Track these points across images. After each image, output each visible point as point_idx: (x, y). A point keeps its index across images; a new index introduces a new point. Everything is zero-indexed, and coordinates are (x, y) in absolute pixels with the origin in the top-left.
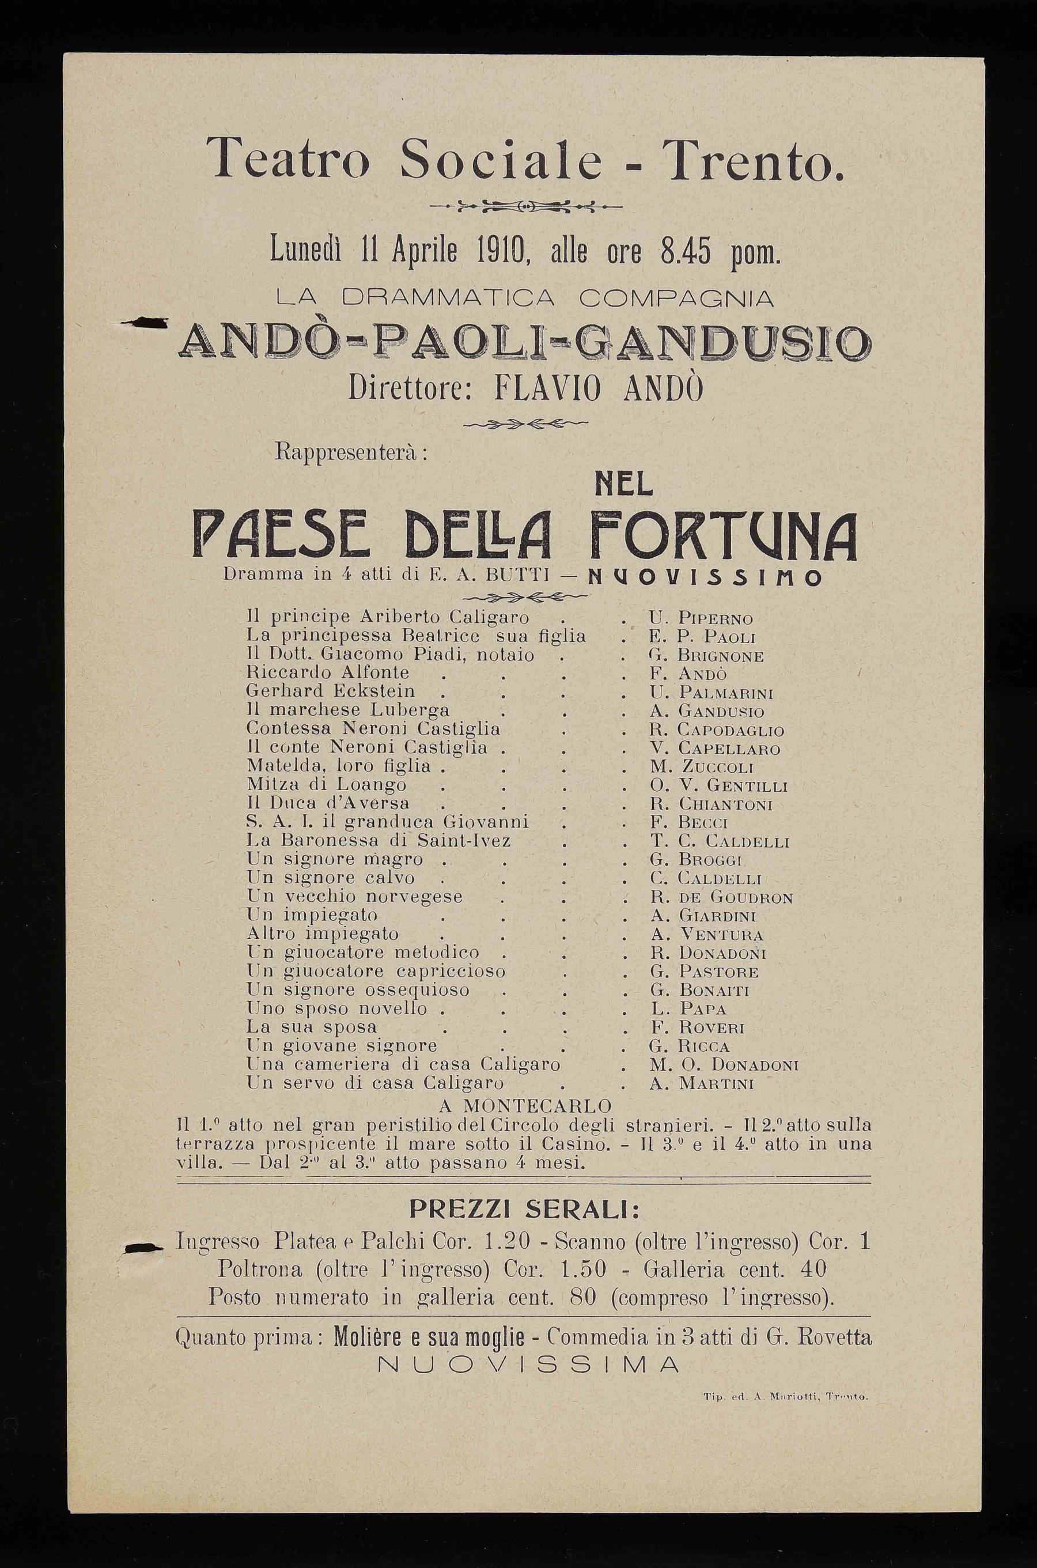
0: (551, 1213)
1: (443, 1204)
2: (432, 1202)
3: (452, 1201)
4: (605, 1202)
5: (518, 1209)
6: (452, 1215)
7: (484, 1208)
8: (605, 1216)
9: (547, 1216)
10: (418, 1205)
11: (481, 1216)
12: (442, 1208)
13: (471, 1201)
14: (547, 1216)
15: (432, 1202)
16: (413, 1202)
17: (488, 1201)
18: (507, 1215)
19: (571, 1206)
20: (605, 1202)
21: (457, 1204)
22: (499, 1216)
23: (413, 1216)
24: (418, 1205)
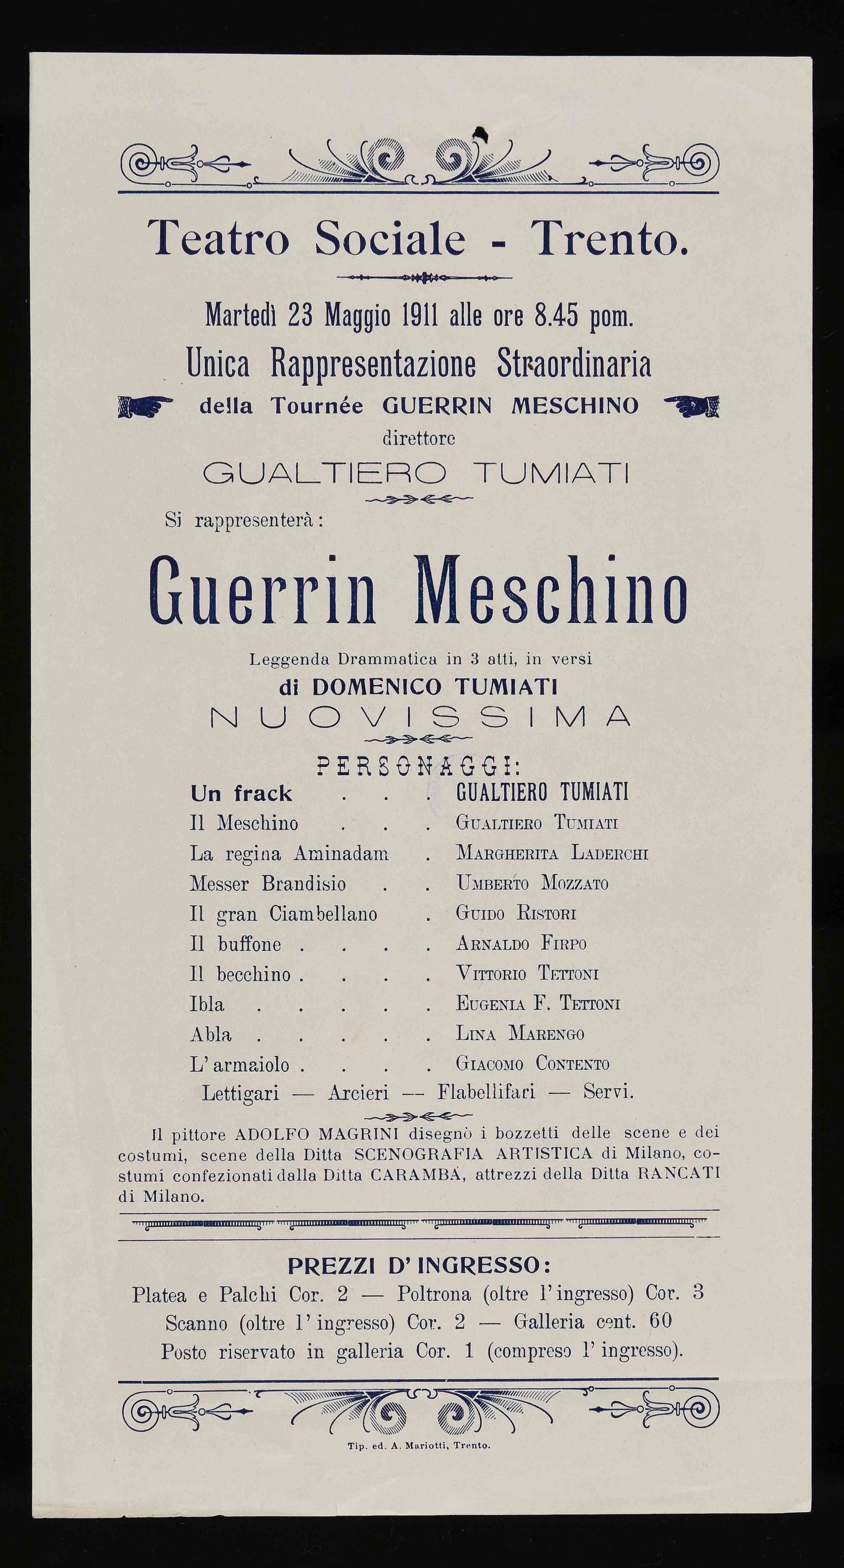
2: (307, 1260)
3: (325, 1260)
6: (325, 1272)
7: (353, 1266)
10: (295, 1263)
11: (350, 1272)
13: (341, 1259)
15: (307, 1260)
16: (291, 1260)
17: (356, 1259)
18: (372, 1271)
21: (329, 1262)
22: (365, 1272)
23: (291, 1272)
24: (295, 1263)
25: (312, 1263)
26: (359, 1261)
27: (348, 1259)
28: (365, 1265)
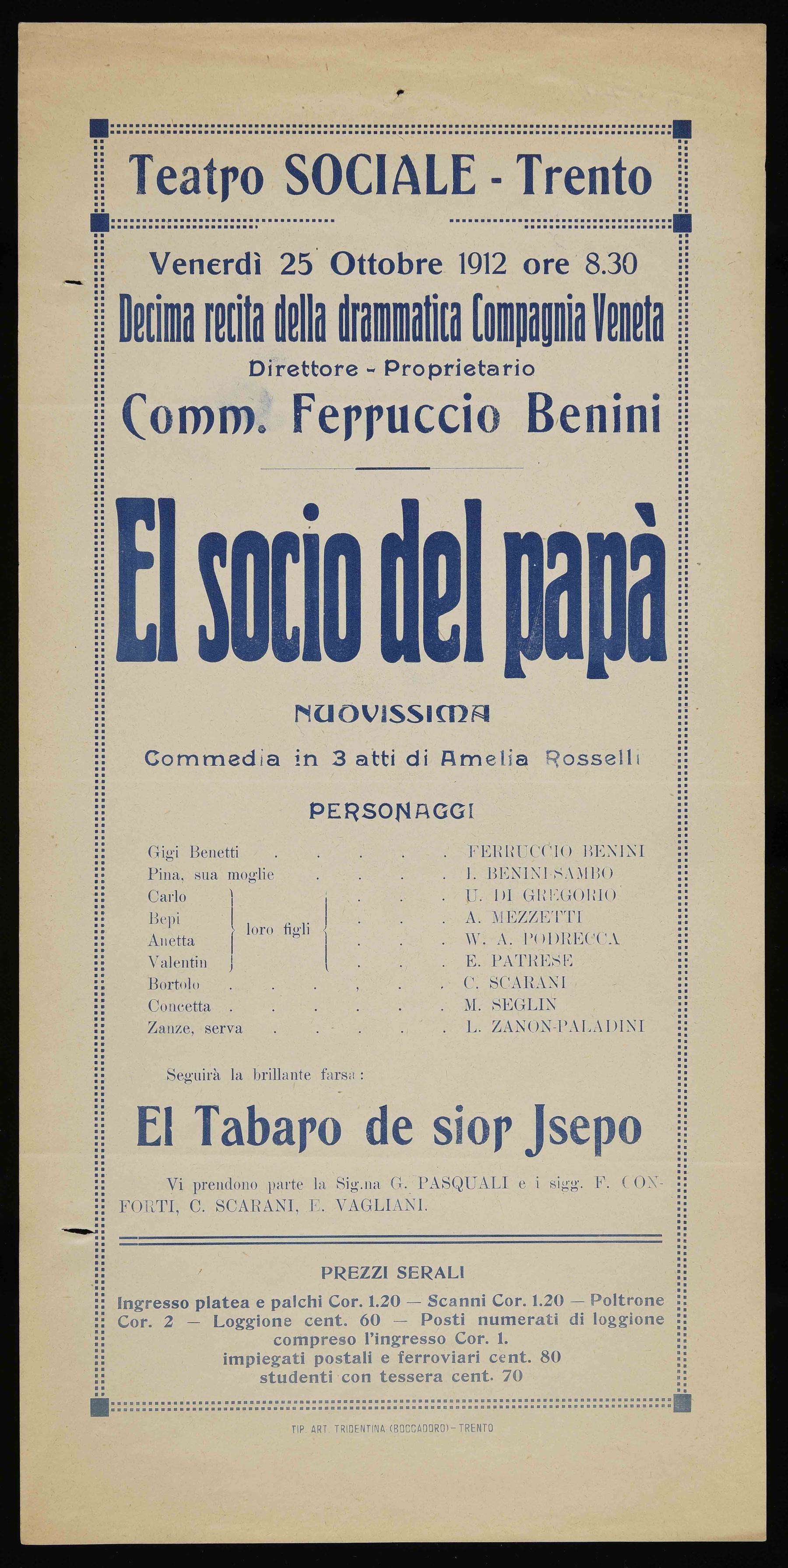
0: (414, 1275)
1: (344, 1271)
2: (336, 1268)
3: (350, 1268)
4: (450, 1268)
5: (393, 1272)
6: (350, 1277)
7: (371, 1273)
8: (450, 1277)
9: (410, 1277)
10: (327, 1271)
12: (344, 1271)
14: (410, 1277)
15: (336, 1268)
18: (385, 1277)
19: (427, 1270)
20: (450, 1268)
21: (353, 1270)
23: (324, 1278)
25: (340, 1271)
26: (376, 1269)
27: (368, 1268)
28: (381, 1272)
